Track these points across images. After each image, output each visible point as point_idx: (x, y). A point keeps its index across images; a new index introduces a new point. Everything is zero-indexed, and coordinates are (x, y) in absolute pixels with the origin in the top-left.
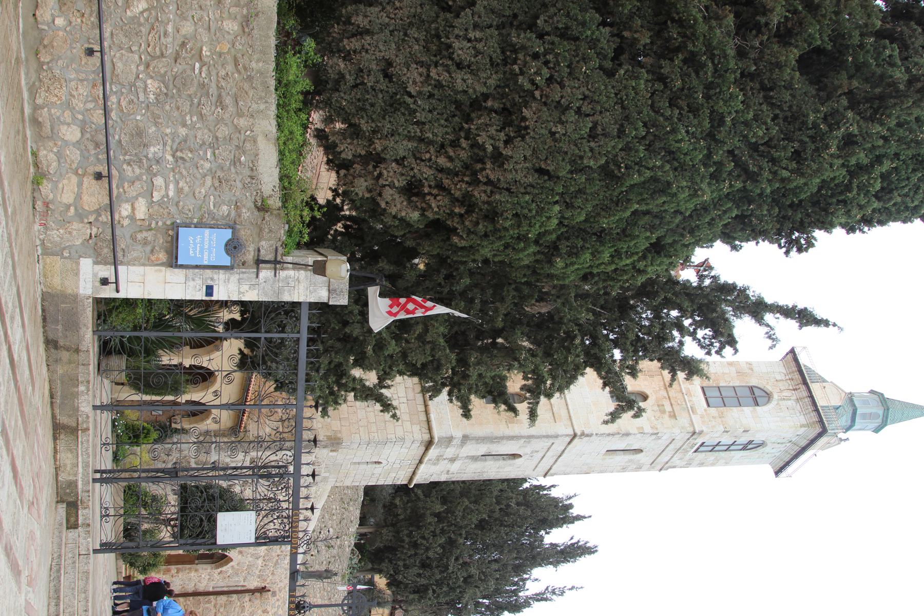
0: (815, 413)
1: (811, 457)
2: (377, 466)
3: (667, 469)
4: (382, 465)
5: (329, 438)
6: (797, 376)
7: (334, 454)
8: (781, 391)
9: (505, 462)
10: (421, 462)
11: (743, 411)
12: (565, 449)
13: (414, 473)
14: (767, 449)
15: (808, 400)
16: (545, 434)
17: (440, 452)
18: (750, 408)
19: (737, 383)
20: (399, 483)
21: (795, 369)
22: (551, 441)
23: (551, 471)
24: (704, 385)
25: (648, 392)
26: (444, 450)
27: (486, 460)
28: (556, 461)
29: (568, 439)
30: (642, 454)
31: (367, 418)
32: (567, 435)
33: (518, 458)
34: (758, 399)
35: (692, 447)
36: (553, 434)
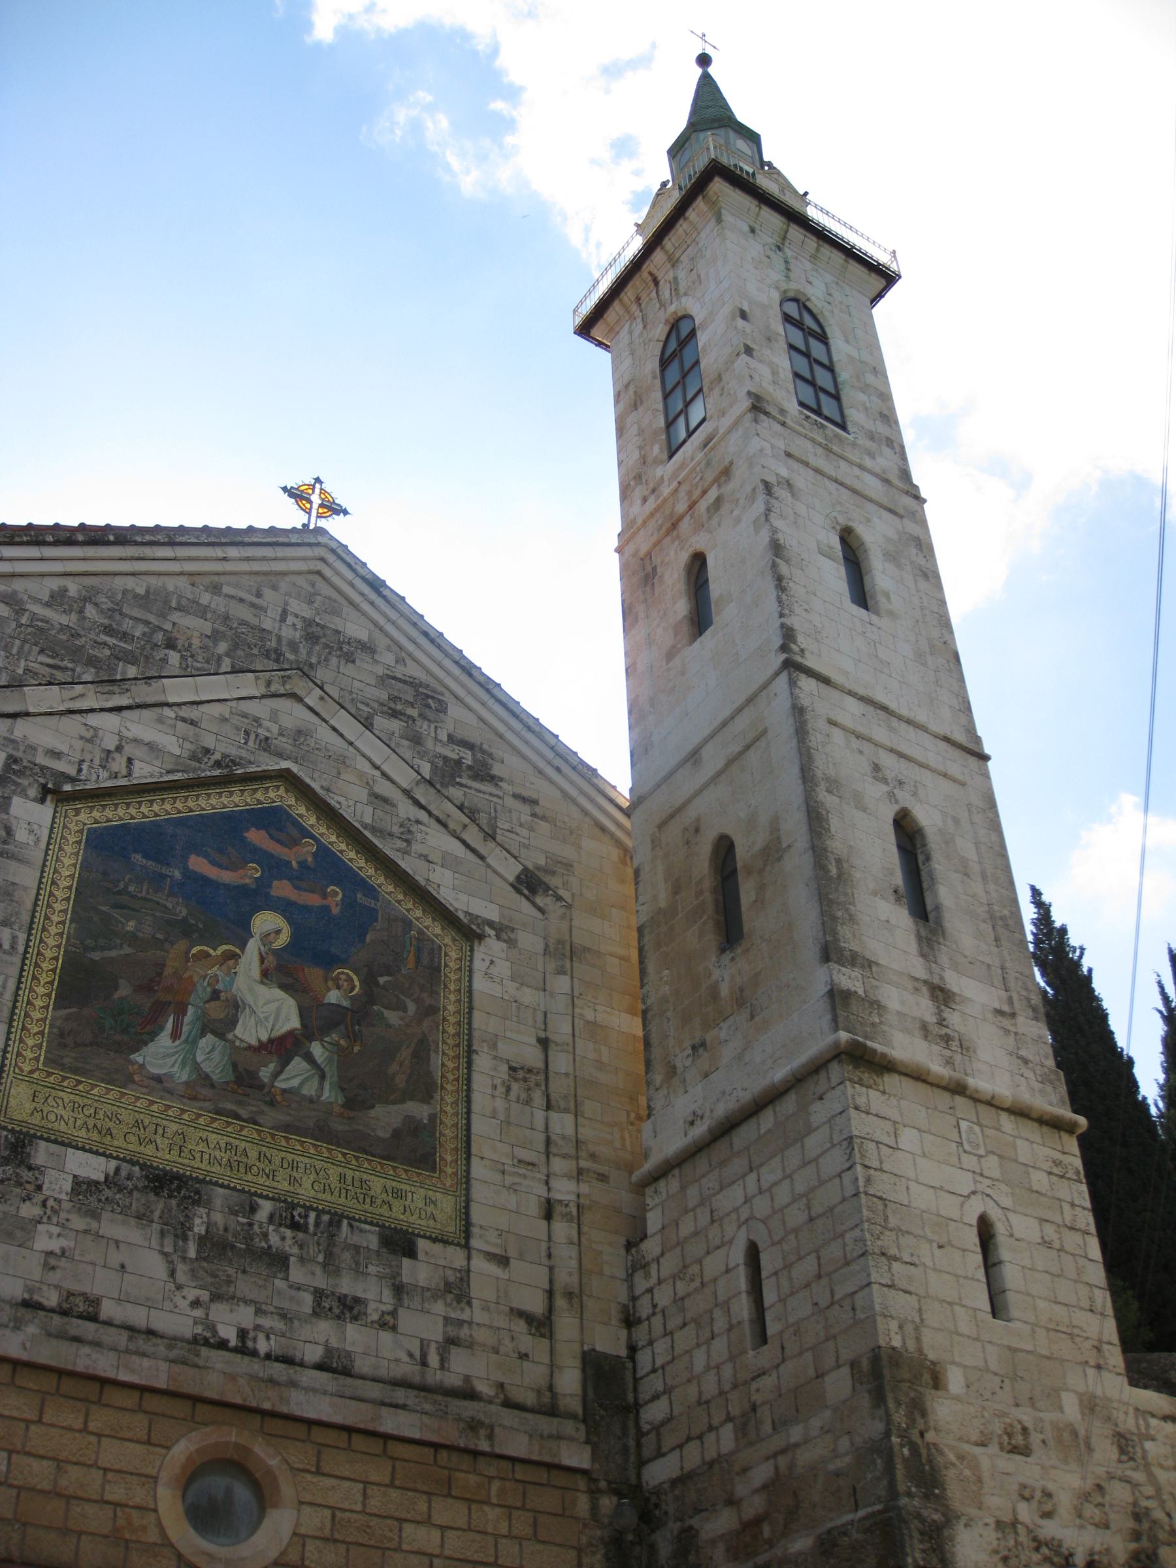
0: (691, 214)
2: (1000, 1229)
3: (916, 488)
4: (994, 1214)
5: (879, 1397)
6: (629, 294)
7: (955, 1380)
10: (958, 1089)
12: (851, 693)
13: (1019, 1112)
14: (816, 294)
16: (794, 743)
17: (906, 1031)
18: (699, 334)
19: (659, 395)
20: (1078, 1163)
21: (616, 304)
23: (960, 737)
24: (665, 456)
25: (684, 557)
27: (937, 908)
28: (909, 722)
29: (807, 685)
30: (861, 530)
31: (808, 1285)
32: (793, 683)
33: (914, 821)
34: (684, 334)
35: (823, 426)
36: (791, 721)
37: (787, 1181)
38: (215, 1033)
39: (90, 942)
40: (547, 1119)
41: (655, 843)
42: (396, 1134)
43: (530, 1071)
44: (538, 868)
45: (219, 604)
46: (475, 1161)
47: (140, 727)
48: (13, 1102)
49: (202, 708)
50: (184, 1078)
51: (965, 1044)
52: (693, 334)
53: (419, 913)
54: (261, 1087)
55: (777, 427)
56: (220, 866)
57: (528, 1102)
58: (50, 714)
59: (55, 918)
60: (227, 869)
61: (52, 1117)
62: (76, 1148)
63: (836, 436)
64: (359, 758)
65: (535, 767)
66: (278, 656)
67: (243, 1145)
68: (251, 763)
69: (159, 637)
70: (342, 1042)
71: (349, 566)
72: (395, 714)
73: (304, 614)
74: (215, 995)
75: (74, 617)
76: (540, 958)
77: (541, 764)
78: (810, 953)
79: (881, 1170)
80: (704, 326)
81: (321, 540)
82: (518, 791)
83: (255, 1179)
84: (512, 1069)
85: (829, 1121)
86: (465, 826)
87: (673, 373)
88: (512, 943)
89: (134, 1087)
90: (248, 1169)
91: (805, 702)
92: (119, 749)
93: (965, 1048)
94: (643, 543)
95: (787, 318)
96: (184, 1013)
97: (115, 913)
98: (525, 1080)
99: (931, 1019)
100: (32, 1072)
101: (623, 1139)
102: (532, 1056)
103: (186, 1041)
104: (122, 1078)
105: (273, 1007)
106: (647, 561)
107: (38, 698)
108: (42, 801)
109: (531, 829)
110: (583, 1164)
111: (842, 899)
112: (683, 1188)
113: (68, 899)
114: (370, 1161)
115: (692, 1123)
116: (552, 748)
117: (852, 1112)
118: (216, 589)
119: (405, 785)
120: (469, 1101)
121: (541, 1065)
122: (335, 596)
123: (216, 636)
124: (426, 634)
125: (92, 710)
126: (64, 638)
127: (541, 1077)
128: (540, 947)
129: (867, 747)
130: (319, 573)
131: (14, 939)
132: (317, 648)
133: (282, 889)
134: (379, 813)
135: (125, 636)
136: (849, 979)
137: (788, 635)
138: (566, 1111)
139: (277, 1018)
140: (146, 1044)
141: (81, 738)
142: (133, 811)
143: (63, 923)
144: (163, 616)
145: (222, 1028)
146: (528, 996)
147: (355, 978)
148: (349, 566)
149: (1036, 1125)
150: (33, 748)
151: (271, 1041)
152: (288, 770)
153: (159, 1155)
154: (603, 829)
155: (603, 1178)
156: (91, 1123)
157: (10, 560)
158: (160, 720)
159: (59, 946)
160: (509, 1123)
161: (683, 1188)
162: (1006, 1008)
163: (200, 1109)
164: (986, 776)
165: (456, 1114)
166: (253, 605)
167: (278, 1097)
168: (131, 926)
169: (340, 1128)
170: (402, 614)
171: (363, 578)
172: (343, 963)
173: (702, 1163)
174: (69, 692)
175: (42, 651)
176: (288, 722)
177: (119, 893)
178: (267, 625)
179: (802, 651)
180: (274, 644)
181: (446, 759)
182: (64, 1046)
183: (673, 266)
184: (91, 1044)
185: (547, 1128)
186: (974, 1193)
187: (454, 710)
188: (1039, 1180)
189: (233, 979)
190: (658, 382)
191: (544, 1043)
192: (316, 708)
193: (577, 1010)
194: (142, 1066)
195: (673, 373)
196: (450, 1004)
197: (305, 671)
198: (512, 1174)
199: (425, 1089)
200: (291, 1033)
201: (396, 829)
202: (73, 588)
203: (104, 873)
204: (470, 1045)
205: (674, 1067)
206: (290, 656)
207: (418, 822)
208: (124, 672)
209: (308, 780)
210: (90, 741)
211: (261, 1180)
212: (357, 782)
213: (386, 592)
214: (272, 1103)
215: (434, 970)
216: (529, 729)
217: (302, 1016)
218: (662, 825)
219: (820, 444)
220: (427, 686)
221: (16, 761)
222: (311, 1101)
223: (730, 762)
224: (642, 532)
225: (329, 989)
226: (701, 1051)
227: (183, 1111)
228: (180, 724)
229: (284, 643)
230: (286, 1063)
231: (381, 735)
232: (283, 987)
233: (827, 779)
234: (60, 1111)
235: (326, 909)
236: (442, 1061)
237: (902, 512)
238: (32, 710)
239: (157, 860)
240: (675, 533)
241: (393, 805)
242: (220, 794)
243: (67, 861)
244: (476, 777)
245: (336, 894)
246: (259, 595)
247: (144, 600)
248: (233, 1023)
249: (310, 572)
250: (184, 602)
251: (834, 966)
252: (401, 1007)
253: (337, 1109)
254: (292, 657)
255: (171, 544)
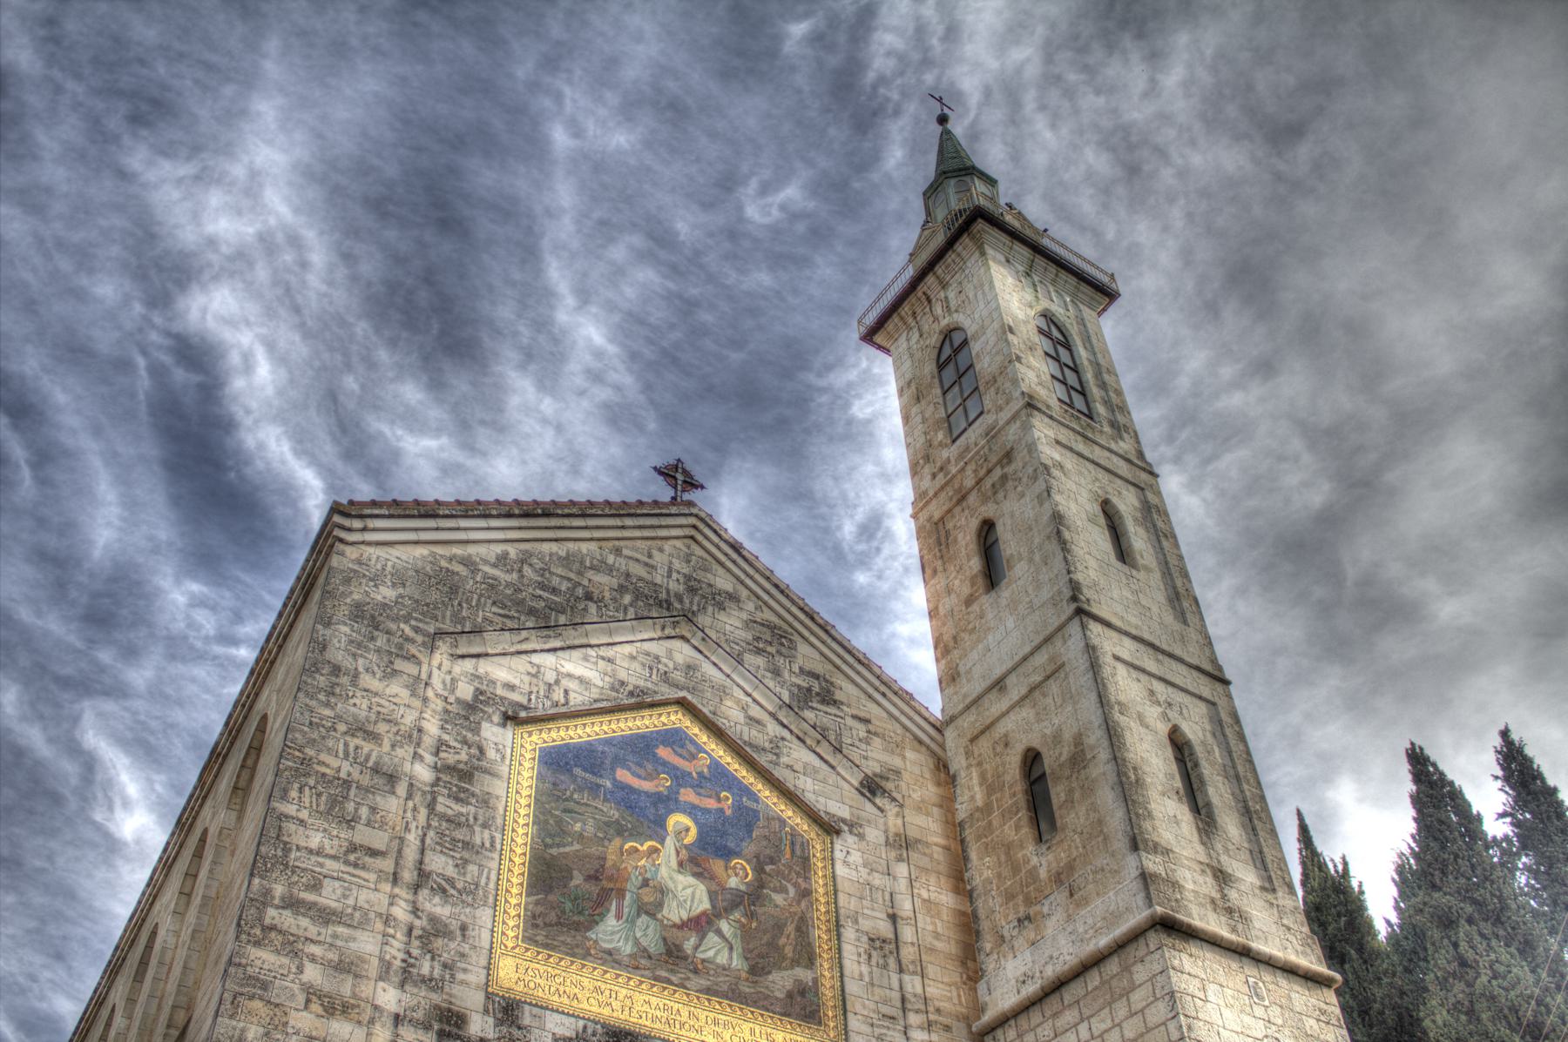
0: (958, 247)
1: (1053, 239)
3: (1150, 465)
6: (906, 309)
8: (936, 319)
9: (1203, 763)
11: (977, 354)
12: (1127, 634)
14: (1057, 309)
15: (939, 269)
16: (1090, 675)
17: (1201, 905)
18: (972, 344)
19: (938, 391)
20: (1338, 1011)
21: (895, 319)
22: (1107, 659)
23: (1207, 667)
25: (974, 523)
26: (1190, 896)
27: (1208, 805)
28: (1171, 656)
29: (1095, 628)
30: (1115, 500)
32: (1084, 627)
33: (1183, 735)
37: (1117, 1028)
38: (647, 913)
39: (548, 841)
40: (900, 980)
41: (968, 754)
42: (790, 995)
43: (884, 941)
44: (875, 775)
45: (621, 563)
46: (850, 1016)
47: (572, 664)
48: (502, 974)
49: (618, 648)
50: (628, 949)
51: (1244, 915)
52: (965, 342)
53: (790, 813)
54: (685, 958)
55: (1047, 420)
56: (639, 777)
57: (885, 966)
58: (504, 654)
59: (521, 821)
60: (645, 779)
61: (532, 985)
62: (552, 1010)
63: (1088, 425)
64: (735, 687)
65: (866, 693)
66: (669, 604)
67: (676, 1006)
68: (656, 692)
69: (580, 592)
70: (743, 920)
71: (715, 532)
72: (759, 651)
73: (684, 571)
74: (646, 883)
75: (515, 576)
76: (883, 848)
77: (871, 690)
78: (1120, 843)
79: (1197, 1018)
80: (976, 337)
81: (694, 511)
82: (855, 712)
83: (688, 1034)
84: (872, 940)
85: (1151, 979)
86: (818, 742)
87: (949, 374)
88: (861, 837)
89: (591, 959)
90: (682, 1025)
91: (1095, 641)
92: (557, 682)
93: (1244, 918)
94: (936, 510)
95: (1041, 331)
96: (623, 897)
97: (566, 818)
98: (881, 948)
99: (1217, 896)
100: (514, 948)
101: (959, 996)
102: (885, 928)
103: (627, 920)
104: (582, 952)
105: (689, 891)
106: (941, 525)
107: (496, 642)
108: (504, 725)
109: (868, 744)
110: (932, 1017)
111: (1141, 799)
112: (1020, 1036)
113: (529, 806)
114: (772, 1018)
115: (1024, 982)
116: (878, 677)
117: (1171, 971)
118: (618, 552)
119: (770, 708)
120: (841, 967)
121: (891, 936)
122: (706, 556)
123: (622, 589)
124: (776, 586)
125: (535, 651)
126: (508, 592)
127: (893, 946)
128: (882, 840)
129: (1144, 678)
130: (692, 537)
131: (493, 839)
132: (697, 599)
133: (688, 795)
134: (754, 733)
135: (554, 591)
136: (1153, 864)
137: (1075, 587)
138: (914, 973)
139: (692, 901)
140: (597, 923)
141: (529, 673)
142: (571, 733)
143: (527, 825)
144: (580, 573)
145: (650, 910)
146: (877, 880)
147: (748, 867)
148: (715, 532)
149: (1303, 981)
150: (493, 682)
151: (690, 920)
152: (684, 698)
153: (615, 1015)
154: (921, 742)
155: (947, 1028)
156: (562, 989)
157: (466, 529)
158: (586, 658)
159: (526, 844)
160: (873, 985)
161: (1020, 1036)
162: (1267, 885)
163: (642, 976)
164: (1229, 696)
165: (832, 977)
166: (646, 564)
167: (700, 966)
168: (578, 827)
169: (747, 990)
170: (757, 570)
171: (726, 541)
172: (738, 855)
173: (1035, 1016)
174: (516, 638)
175: (494, 603)
176: (679, 658)
177: (567, 800)
178: (658, 580)
179: (1088, 600)
180: (663, 596)
181: (799, 686)
182: (536, 926)
183: (943, 288)
184: (556, 924)
185: (901, 988)
186: (1266, 1036)
187: (803, 648)
188: (1311, 1024)
189: (657, 870)
190: (936, 381)
191: (893, 918)
192: (701, 648)
193: (916, 891)
194: (596, 942)
195: (949, 374)
196: (819, 885)
197: (689, 617)
198: (878, 1026)
199: (808, 957)
200: (704, 913)
201: (767, 745)
202: (512, 551)
203: (554, 784)
204: (837, 921)
205: (1002, 936)
206: (679, 606)
207: (783, 739)
208: (556, 621)
209: (700, 706)
210: (535, 676)
211: (693, 1035)
212: (735, 706)
213: (745, 553)
214: (696, 971)
215: (805, 862)
216: (860, 661)
217: (711, 900)
218: (973, 740)
219: (1079, 433)
220: (780, 628)
221: (481, 693)
222: (724, 969)
223: (1032, 690)
224: (934, 502)
225: (729, 876)
226: (1026, 923)
227: (630, 979)
228: (600, 662)
229: (672, 594)
230: (702, 939)
231: (751, 669)
232: (696, 875)
233: (1119, 703)
234: (538, 980)
235: (721, 810)
236: (820, 934)
237: (1142, 485)
238: (490, 651)
239: (594, 774)
240: (964, 504)
241: (764, 726)
242: (635, 718)
243: (526, 774)
244: (823, 702)
245: (728, 798)
246: (650, 556)
247: (567, 560)
248: (660, 905)
249: (685, 537)
250: (595, 562)
251: (1143, 854)
252: (783, 890)
253: (744, 975)
254: (679, 606)
255: (584, 516)
